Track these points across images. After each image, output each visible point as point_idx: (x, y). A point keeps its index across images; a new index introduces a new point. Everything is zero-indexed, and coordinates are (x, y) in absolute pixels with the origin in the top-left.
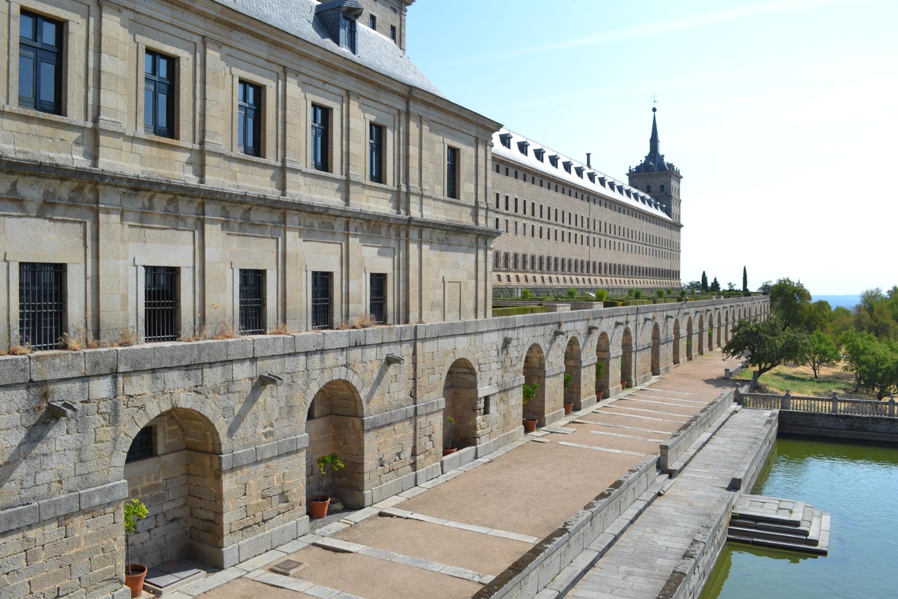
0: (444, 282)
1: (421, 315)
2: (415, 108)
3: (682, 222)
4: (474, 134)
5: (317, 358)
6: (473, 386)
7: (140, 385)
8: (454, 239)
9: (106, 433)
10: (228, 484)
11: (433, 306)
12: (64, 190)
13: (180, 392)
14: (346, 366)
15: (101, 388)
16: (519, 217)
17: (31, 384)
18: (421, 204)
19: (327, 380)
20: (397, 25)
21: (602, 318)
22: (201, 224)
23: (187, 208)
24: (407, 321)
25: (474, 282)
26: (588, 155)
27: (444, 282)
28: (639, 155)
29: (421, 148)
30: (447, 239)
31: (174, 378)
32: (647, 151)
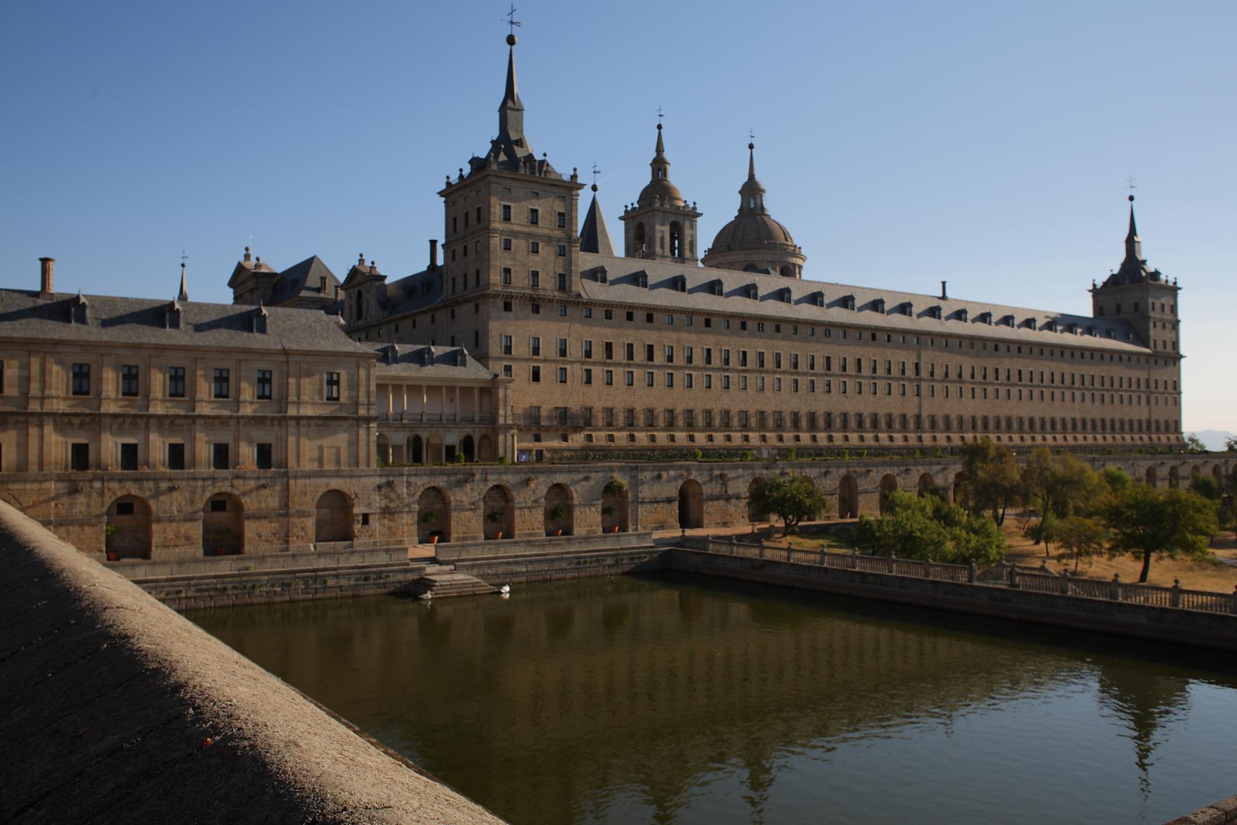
2: (291, 358)
3: (1183, 351)
5: (210, 482)
6: (353, 506)
7: (114, 485)
8: (331, 423)
9: (100, 500)
10: (154, 527)
12: (87, 419)
13: (133, 489)
14: (232, 486)
15: (98, 485)
16: (767, 372)
17: (70, 481)
19: (216, 491)
22: (147, 427)
23: (139, 421)
26: (944, 283)
28: (1113, 262)
31: (129, 484)
32: (1122, 256)
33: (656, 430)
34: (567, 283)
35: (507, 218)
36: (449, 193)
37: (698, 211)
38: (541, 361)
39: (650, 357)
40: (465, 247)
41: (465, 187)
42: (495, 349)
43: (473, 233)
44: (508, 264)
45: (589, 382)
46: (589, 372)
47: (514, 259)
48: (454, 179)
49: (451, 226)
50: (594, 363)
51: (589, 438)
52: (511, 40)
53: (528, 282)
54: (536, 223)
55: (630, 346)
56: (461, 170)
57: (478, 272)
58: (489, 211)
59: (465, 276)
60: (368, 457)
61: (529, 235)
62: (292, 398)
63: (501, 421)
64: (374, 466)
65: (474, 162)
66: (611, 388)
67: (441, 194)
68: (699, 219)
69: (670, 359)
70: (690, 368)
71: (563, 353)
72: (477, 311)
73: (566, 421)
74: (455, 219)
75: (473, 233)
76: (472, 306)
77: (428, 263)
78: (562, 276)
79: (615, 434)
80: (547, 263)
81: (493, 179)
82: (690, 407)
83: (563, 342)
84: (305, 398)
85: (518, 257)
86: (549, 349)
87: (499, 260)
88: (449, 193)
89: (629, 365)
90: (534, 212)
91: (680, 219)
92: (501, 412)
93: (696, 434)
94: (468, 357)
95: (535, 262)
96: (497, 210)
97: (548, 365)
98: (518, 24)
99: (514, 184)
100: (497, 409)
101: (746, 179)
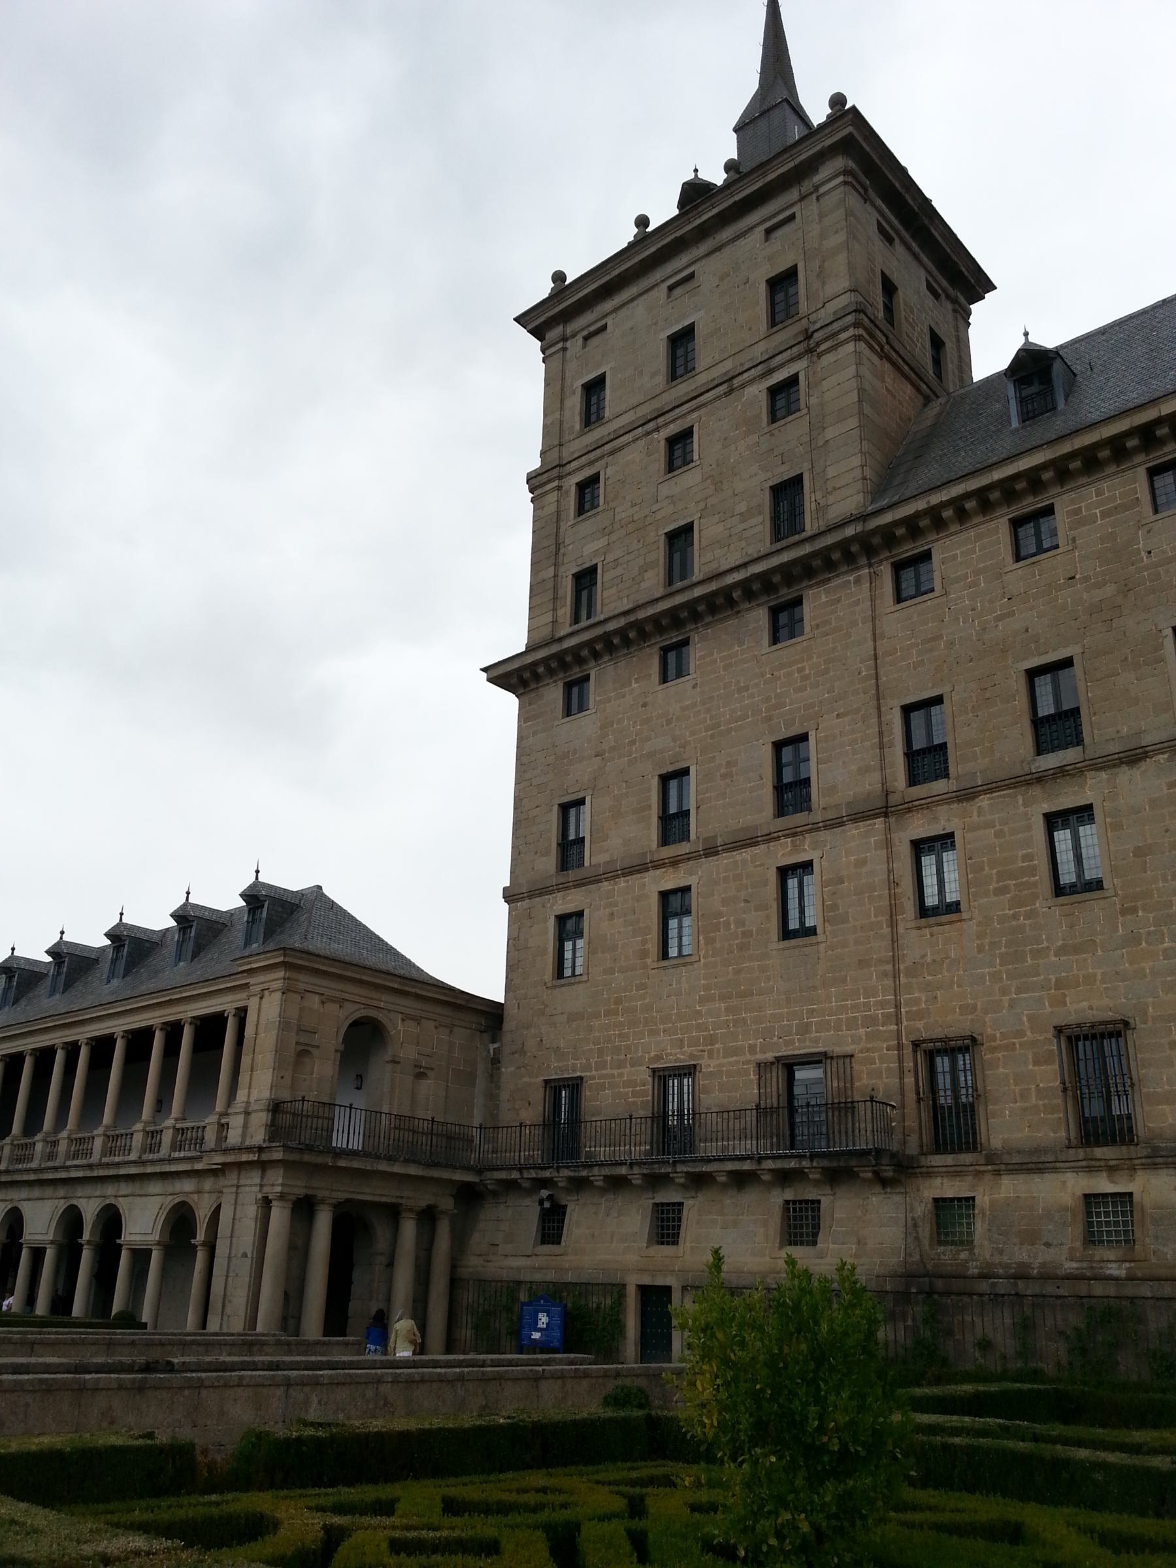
97: (725, 859)
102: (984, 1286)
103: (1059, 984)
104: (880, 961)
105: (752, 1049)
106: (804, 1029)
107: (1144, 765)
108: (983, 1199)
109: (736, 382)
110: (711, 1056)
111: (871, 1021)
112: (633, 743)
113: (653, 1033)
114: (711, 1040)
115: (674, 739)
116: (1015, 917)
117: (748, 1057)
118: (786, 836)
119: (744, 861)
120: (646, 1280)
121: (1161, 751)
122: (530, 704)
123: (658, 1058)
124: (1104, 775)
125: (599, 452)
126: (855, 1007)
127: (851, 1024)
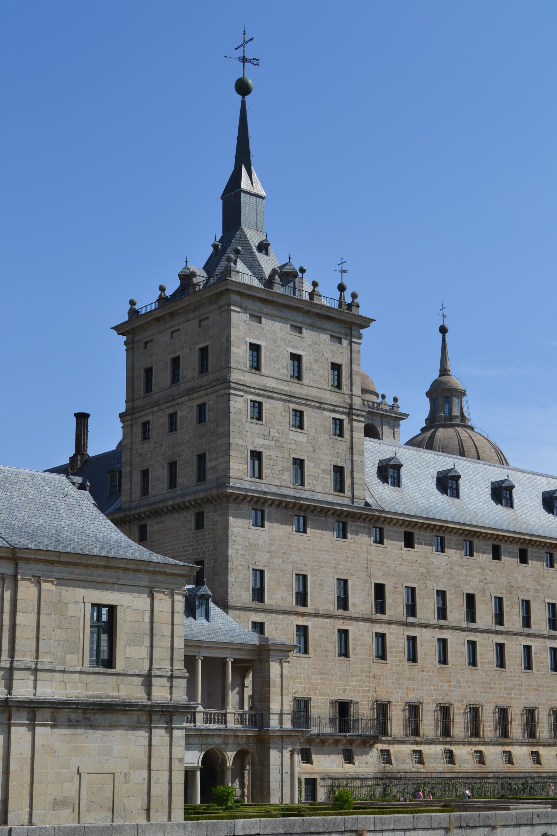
0: (79, 773)
1: (31, 815)
4: (147, 584)
8: (99, 718)
11: (57, 804)
18: (35, 680)
20: (343, 360)
21: (494, 828)
24: (5, 823)
25: (145, 773)
27: (79, 773)
29: (39, 613)
30: (85, 718)
33: (485, 743)
34: (348, 482)
35: (257, 366)
36: (135, 328)
37: (401, 410)
38: (309, 615)
39: (471, 616)
40: (173, 418)
41: (172, 315)
42: (239, 590)
43: (192, 390)
44: (259, 444)
45: (382, 656)
46: (381, 637)
47: (265, 436)
48: (147, 301)
49: (141, 384)
50: (390, 623)
51: (386, 756)
52: (243, 88)
53: (288, 477)
54: (299, 377)
55: (442, 594)
56: (162, 289)
57: (201, 458)
58: (228, 351)
59: (173, 466)
60: (483, 802)
61: (289, 397)
62: (25, 657)
63: (274, 723)
64: (178, 814)
65: (186, 278)
66: (415, 668)
67: (120, 329)
68: (401, 422)
69: (499, 619)
70: (529, 635)
71: (343, 602)
72: (200, 524)
73: (348, 729)
74: (149, 372)
75: (192, 390)
76: (190, 516)
77: (72, 452)
78: (339, 471)
79: (424, 748)
80: (319, 447)
81: (234, 298)
82: (530, 705)
83: (343, 584)
84: (46, 660)
85: (274, 433)
86: (322, 597)
87: (244, 435)
88: (135, 328)
89: (441, 627)
90: (296, 358)
91: (377, 423)
92: (275, 706)
93: (542, 751)
94: (212, 605)
95: (299, 443)
96: (240, 354)
97: (321, 620)
98: (255, 62)
99: (266, 309)
100: (267, 700)
101: (435, 375)
102: (399, 775)
103: (407, 689)
104: (367, 672)
105: (329, 694)
106: (345, 690)
107: (428, 629)
108: (391, 751)
109: (323, 406)
110: (315, 694)
111: (363, 691)
112: (284, 553)
113: (294, 682)
114: (315, 689)
115: (301, 560)
116: (399, 666)
117: (327, 697)
118: (342, 618)
119: (327, 622)
120: (308, 776)
121: (431, 626)
122: (235, 510)
123: (296, 693)
124: (419, 628)
125: (264, 393)
126: (360, 685)
127: (358, 691)
